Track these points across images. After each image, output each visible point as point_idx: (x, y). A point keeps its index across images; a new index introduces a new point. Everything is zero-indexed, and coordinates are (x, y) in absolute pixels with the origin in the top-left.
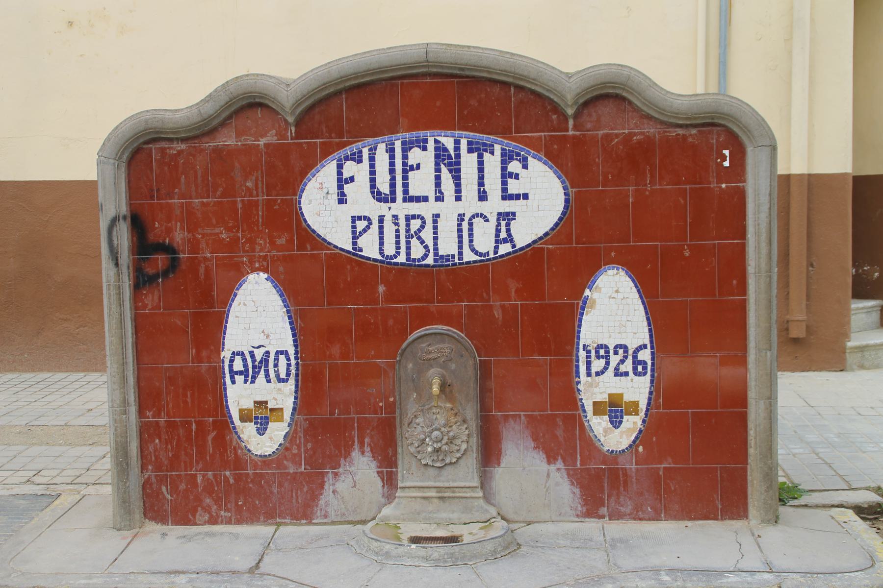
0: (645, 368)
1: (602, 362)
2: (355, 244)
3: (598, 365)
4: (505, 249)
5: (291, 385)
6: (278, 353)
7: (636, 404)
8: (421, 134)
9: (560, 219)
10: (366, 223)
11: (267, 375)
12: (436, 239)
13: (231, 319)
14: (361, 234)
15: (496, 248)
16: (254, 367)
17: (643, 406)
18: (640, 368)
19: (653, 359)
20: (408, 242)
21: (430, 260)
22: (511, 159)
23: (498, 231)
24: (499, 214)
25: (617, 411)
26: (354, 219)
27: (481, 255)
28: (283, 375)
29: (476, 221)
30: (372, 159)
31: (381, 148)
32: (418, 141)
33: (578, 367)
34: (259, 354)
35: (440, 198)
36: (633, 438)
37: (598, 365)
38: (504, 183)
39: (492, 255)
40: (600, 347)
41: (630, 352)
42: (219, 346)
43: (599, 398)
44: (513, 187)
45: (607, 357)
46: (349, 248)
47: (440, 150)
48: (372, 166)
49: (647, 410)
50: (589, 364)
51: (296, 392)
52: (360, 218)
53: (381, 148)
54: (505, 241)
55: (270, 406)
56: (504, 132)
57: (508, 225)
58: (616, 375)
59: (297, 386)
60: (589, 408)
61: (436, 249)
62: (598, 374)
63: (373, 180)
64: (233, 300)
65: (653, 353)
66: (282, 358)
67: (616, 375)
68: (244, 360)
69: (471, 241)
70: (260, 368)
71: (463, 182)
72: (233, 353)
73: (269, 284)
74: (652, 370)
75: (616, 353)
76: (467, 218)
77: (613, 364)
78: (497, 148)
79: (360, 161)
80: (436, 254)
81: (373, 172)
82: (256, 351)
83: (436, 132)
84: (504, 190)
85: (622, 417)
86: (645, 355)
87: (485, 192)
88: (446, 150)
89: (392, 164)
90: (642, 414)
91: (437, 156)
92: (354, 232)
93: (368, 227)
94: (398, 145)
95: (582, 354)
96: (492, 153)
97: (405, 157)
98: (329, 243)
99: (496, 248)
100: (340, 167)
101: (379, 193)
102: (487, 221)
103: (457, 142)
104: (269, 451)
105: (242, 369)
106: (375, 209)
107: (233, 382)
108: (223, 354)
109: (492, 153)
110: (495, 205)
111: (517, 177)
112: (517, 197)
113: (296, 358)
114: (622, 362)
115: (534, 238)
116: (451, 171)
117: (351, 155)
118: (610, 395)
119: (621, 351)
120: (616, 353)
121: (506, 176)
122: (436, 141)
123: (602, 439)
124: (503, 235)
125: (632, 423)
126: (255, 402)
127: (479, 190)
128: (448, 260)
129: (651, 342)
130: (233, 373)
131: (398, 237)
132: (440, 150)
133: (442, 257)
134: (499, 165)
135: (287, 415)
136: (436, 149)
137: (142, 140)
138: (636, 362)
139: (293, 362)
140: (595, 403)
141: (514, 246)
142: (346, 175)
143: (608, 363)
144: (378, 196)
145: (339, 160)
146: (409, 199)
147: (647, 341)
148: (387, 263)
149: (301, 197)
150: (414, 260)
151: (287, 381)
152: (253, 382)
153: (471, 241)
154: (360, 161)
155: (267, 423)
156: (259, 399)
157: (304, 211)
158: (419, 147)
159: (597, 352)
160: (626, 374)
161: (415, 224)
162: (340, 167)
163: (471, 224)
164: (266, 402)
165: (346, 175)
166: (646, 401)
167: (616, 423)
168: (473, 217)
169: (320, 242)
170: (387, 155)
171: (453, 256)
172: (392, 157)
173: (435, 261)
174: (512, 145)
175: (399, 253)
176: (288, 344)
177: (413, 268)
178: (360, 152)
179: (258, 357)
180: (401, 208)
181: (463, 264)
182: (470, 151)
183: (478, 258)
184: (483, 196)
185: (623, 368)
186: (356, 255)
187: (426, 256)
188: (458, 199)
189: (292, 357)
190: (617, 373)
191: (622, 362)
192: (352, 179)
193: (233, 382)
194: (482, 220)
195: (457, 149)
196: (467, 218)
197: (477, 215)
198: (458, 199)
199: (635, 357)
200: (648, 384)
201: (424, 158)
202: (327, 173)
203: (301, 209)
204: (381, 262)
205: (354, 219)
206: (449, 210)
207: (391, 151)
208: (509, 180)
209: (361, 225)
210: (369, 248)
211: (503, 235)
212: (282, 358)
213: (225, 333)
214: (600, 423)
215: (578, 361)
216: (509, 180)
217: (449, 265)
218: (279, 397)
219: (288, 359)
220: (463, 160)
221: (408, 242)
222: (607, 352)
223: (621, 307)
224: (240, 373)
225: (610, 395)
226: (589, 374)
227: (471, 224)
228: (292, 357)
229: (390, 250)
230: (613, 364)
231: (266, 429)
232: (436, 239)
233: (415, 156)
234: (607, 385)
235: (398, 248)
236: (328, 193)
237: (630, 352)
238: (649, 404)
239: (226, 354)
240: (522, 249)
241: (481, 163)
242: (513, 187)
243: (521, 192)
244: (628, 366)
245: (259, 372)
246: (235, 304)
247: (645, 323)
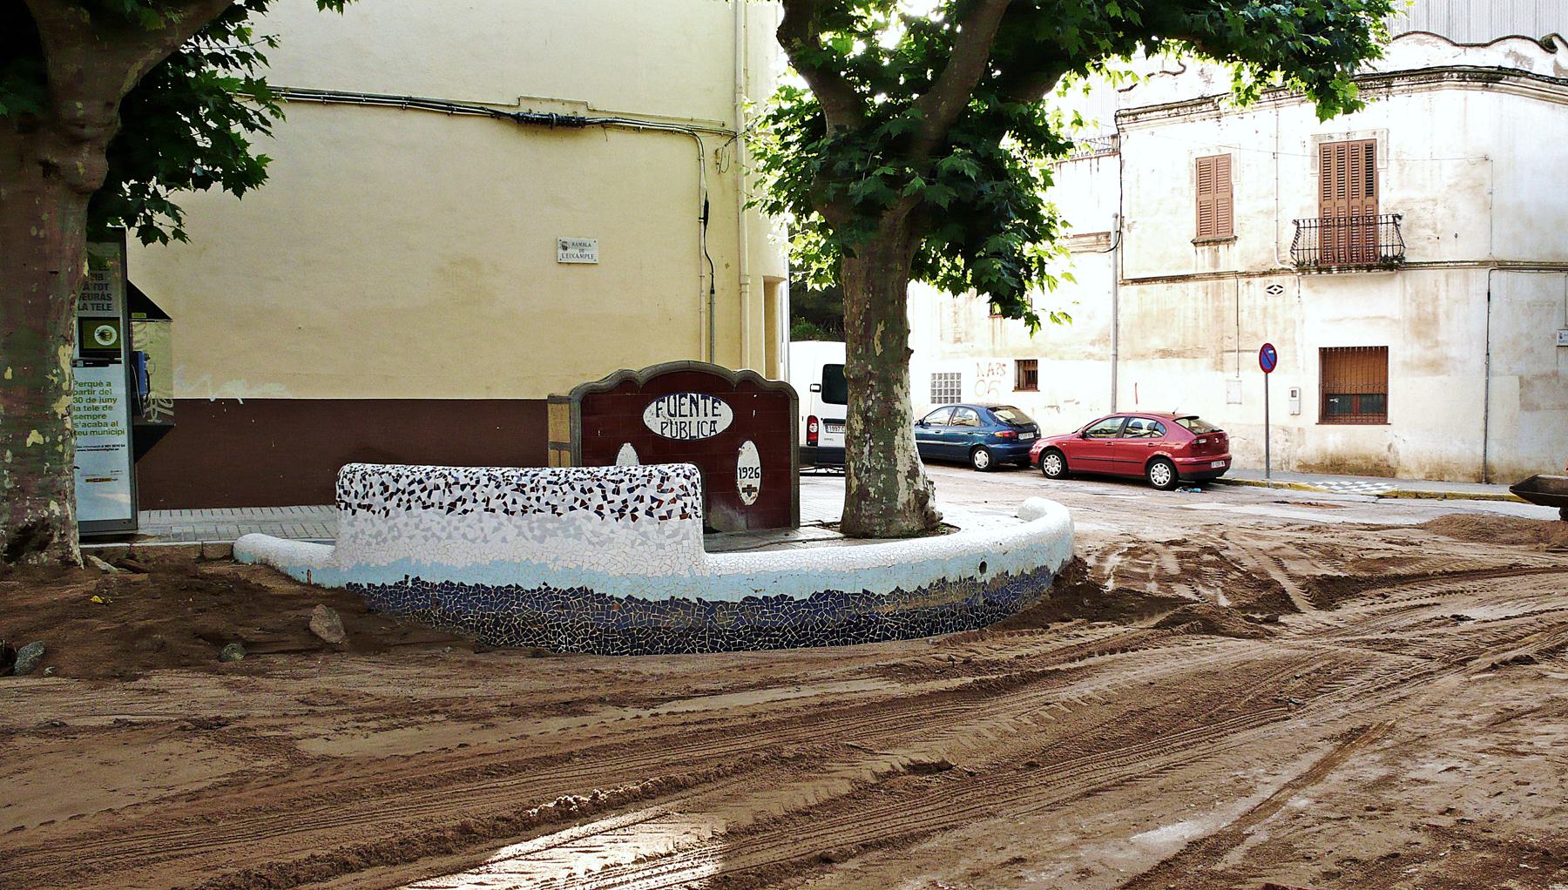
4: (713, 433)
35: (691, 416)
47: (692, 397)
79: (664, 402)
86: (759, 471)
110: (710, 418)
121: (714, 407)
132: (692, 397)
144: (671, 415)
146: (680, 416)
148: (673, 439)
154: (664, 402)
161: (683, 425)
180: (678, 419)
184: (706, 415)
201: (686, 401)
206: (694, 420)
207: (675, 398)
209: (664, 425)
229: (674, 435)
244: (753, 475)
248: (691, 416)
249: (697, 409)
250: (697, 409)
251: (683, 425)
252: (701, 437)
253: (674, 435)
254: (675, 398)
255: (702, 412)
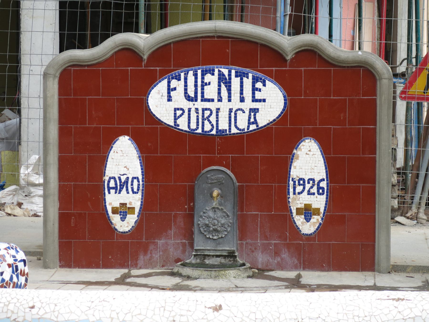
0: (323, 191)
1: (301, 187)
2: (175, 122)
3: (299, 189)
4: (253, 127)
5: (139, 196)
6: (134, 178)
7: (318, 209)
8: (211, 66)
9: (282, 113)
10: (181, 112)
11: (127, 190)
12: (217, 121)
13: (109, 159)
14: (179, 117)
15: (248, 127)
16: (120, 185)
17: (322, 210)
18: (321, 191)
19: (327, 186)
20: (203, 123)
21: (214, 132)
22: (257, 81)
23: (250, 118)
24: (250, 109)
25: (309, 213)
26: (176, 110)
27: (240, 130)
28: (135, 190)
29: (239, 112)
30: (186, 79)
31: (191, 73)
32: (210, 70)
33: (289, 189)
34: (123, 179)
35: (220, 100)
36: (316, 227)
37: (299, 189)
38: (253, 94)
39: (246, 130)
40: (300, 179)
41: (316, 183)
42: (103, 174)
43: (299, 206)
44: (258, 95)
45: (304, 185)
46: (172, 124)
47: (221, 77)
48: (186, 82)
49: (324, 213)
50: (294, 188)
51: (142, 199)
52: (178, 109)
53: (191, 73)
54: (253, 123)
55: (128, 206)
56: (253, 67)
57: (255, 115)
58: (308, 194)
59: (142, 196)
60: (294, 211)
61: (217, 126)
62: (299, 193)
63: (186, 90)
64: (111, 150)
65: (327, 183)
66: (135, 181)
67: (308, 194)
68: (116, 181)
69: (236, 123)
70: (124, 186)
71: (232, 92)
72: (110, 178)
73: (130, 142)
74: (327, 192)
75: (309, 183)
76: (234, 111)
77: (307, 188)
78: (250, 75)
79: (179, 80)
80: (217, 129)
81: (186, 86)
82: (122, 177)
83: (219, 66)
84: (253, 97)
85: (311, 216)
86: (324, 184)
87: (243, 98)
88: (224, 75)
89: (196, 82)
90: (322, 215)
91: (219, 79)
92: (175, 116)
93: (182, 114)
94: (199, 72)
95: (291, 183)
96: (248, 78)
97: (203, 78)
98: (162, 122)
99: (248, 127)
100: (169, 82)
101: (189, 96)
102: (244, 112)
103: (230, 72)
104: (127, 229)
105: (114, 186)
106: (186, 105)
107: (109, 193)
108: (104, 178)
109: (248, 78)
110: (248, 104)
111: (260, 90)
112: (260, 101)
113: (143, 181)
114: (312, 187)
115: (268, 122)
116: (226, 86)
117: (175, 76)
118: (305, 205)
119: (311, 182)
120: (309, 183)
121: (254, 89)
122: (219, 71)
123: (300, 228)
124: (252, 120)
125: (316, 220)
126: (120, 204)
127: (240, 97)
128: (223, 132)
129: (327, 177)
130: (109, 188)
131: (198, 119)
133: (220, 130)
134: (251, 84)
135: (137, 211)
136: (219, 75)
137: (67, 65)
138: (319, 188)
139: (141, 183)
140: (297, 209)
141: (257, 126)
142: (172, 86)
143: (304, 188)
144: (188, 98)
145: (169, 79)
146: (204, 100)
147: (325, 177)
148: (191, 134)
149: (148, 97)
150: (206, 132)
151: (137, 193)
152: (119, 193)
153: (236, 123)
154: (179, 80)
155: (126, 215)
156: (122, 202)
157: (149, 104)
158: (210, 73)
159: (299, 182)
160: (314, 194)
161: (207, 113)
162: (169, 82)
163: (236, 114)
164: (126, 204)
165: (172, 86)
166: (323, 208)
167: (308, 219)
168: (237, 110)
169: (159, 122)
170: (194, 77)
171: (226, 130)
172: (196, 78)
173: (217, 132)
174: (259, 75)
175: (198, 128)
176: (139, 174)
177: (205, 135)
178: (180, 75)
179: (123, 180)
180: (200, 105)
181: (231, 134)
182: (236, 76)
183: (239, 132)
184: (242, 100)
185: (312, 191)
186: (176, 128)
187: (212, 130)
188: (230, 100)
189: (141, 181)
190: (309, 193)
191: (312, 187)
192: (175, 89)
193: (109, 193)
194: (241, 112)
195: (230, 75)
196: (234, 111)
197: (239, 109)
198: (230, 100)
199: (318, 185)
200: (325, 200)
202: (162, 85)
203: (148, 103)
204: (189, 132)
205: (176, 110)
206: (225, 106)
207: (196, 75)
208: (256, 92)
209: (179, 113)
210: (183, 124)
211: (252, 120)
212: (135, 181)
213: (106, 167)
214: (299, 219)
215: (289, 186)
216: (256, 92)
217: (223, 135)
218: (133, 202)
219: (139, 182)
220: (232, 81)
221: (203, 123)
222: (304, 182)
223: (312, 159)
224: (113, 188)
225: (305, 205)
226: (294, 193)
227: (236, 114)
228: (141, 181)
229: (193, 126)
230: (307, 188)
231: (125, 218)
232: (217, 121)
233: (208, 78)
234: (304, 199)
235: (198, 125)
236: (162, 96)
237: (316, 183)
238: (325, 210)
239: (106, 178)
240: (262, 127)
241: (242, 83)
242: (258, 95)
243: (262, 98)
244: (314, 190)
245: (123, 188)
246: (112, 152)
247: (324, 168)
248: (220, 100)
249: (229, 90)
250: (229, 90)
251: (207, 113)
252: (234, 130)
253: (193, 126)
254: (196, 75)
255: (236, 96)
